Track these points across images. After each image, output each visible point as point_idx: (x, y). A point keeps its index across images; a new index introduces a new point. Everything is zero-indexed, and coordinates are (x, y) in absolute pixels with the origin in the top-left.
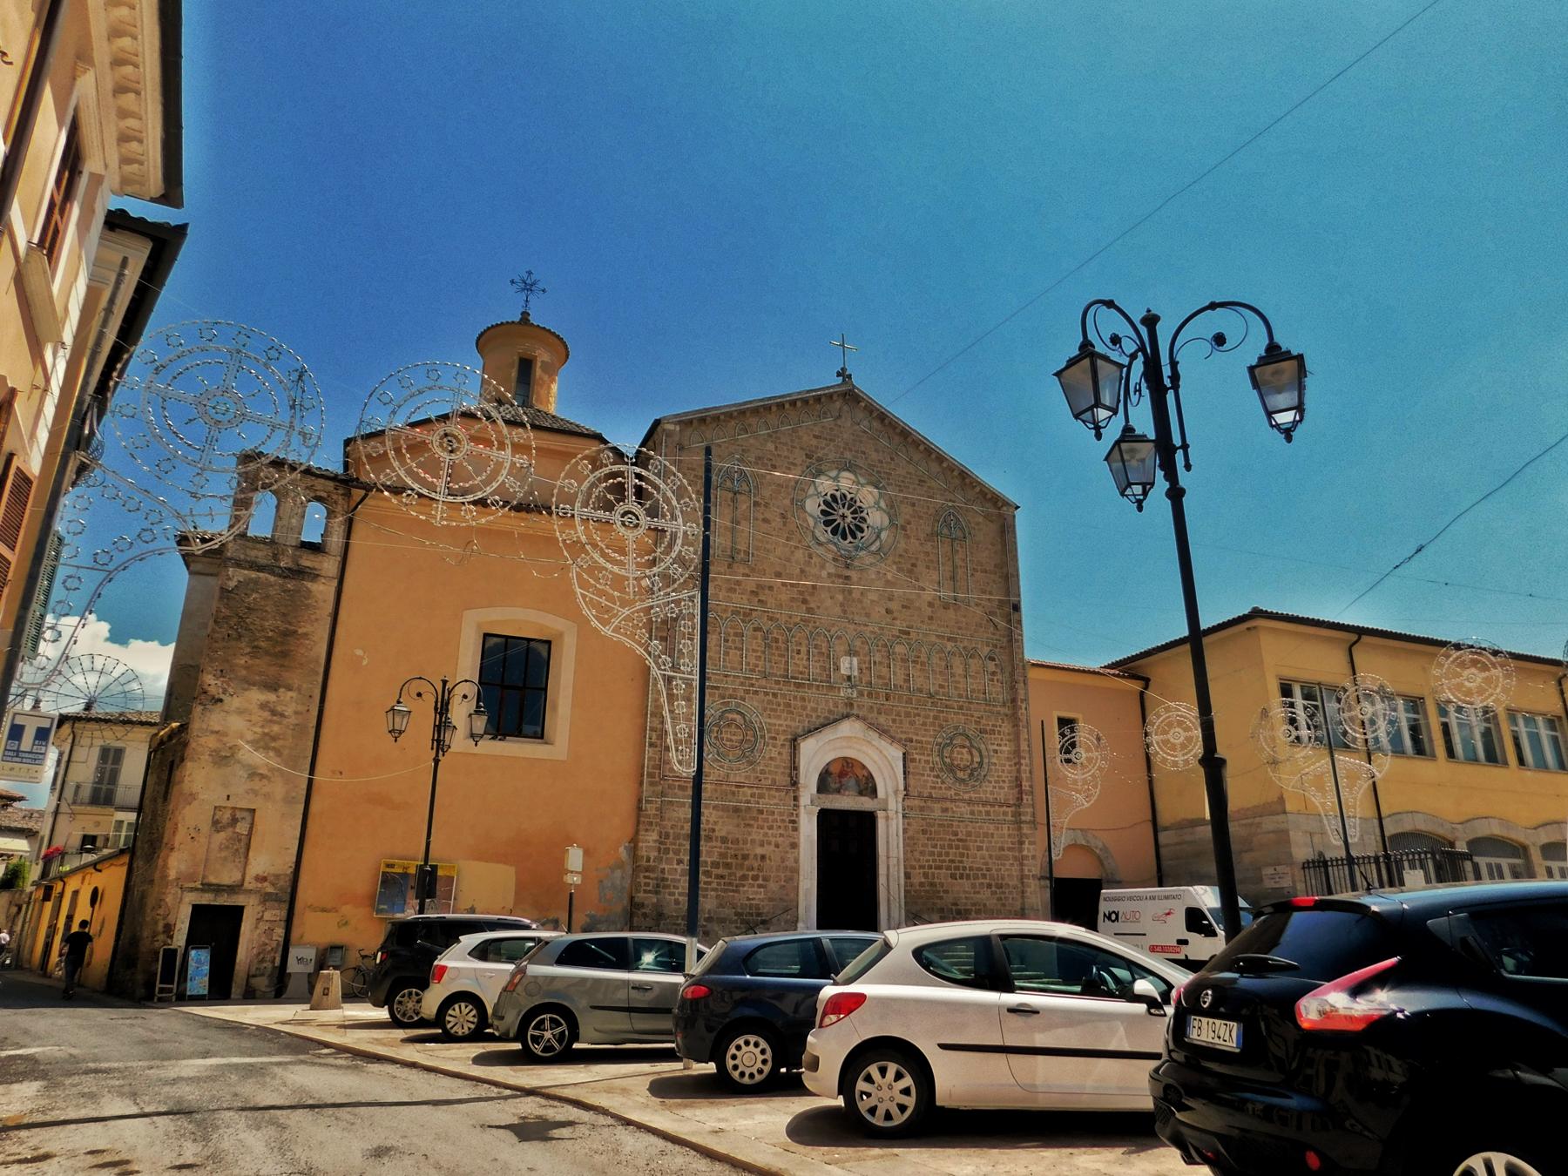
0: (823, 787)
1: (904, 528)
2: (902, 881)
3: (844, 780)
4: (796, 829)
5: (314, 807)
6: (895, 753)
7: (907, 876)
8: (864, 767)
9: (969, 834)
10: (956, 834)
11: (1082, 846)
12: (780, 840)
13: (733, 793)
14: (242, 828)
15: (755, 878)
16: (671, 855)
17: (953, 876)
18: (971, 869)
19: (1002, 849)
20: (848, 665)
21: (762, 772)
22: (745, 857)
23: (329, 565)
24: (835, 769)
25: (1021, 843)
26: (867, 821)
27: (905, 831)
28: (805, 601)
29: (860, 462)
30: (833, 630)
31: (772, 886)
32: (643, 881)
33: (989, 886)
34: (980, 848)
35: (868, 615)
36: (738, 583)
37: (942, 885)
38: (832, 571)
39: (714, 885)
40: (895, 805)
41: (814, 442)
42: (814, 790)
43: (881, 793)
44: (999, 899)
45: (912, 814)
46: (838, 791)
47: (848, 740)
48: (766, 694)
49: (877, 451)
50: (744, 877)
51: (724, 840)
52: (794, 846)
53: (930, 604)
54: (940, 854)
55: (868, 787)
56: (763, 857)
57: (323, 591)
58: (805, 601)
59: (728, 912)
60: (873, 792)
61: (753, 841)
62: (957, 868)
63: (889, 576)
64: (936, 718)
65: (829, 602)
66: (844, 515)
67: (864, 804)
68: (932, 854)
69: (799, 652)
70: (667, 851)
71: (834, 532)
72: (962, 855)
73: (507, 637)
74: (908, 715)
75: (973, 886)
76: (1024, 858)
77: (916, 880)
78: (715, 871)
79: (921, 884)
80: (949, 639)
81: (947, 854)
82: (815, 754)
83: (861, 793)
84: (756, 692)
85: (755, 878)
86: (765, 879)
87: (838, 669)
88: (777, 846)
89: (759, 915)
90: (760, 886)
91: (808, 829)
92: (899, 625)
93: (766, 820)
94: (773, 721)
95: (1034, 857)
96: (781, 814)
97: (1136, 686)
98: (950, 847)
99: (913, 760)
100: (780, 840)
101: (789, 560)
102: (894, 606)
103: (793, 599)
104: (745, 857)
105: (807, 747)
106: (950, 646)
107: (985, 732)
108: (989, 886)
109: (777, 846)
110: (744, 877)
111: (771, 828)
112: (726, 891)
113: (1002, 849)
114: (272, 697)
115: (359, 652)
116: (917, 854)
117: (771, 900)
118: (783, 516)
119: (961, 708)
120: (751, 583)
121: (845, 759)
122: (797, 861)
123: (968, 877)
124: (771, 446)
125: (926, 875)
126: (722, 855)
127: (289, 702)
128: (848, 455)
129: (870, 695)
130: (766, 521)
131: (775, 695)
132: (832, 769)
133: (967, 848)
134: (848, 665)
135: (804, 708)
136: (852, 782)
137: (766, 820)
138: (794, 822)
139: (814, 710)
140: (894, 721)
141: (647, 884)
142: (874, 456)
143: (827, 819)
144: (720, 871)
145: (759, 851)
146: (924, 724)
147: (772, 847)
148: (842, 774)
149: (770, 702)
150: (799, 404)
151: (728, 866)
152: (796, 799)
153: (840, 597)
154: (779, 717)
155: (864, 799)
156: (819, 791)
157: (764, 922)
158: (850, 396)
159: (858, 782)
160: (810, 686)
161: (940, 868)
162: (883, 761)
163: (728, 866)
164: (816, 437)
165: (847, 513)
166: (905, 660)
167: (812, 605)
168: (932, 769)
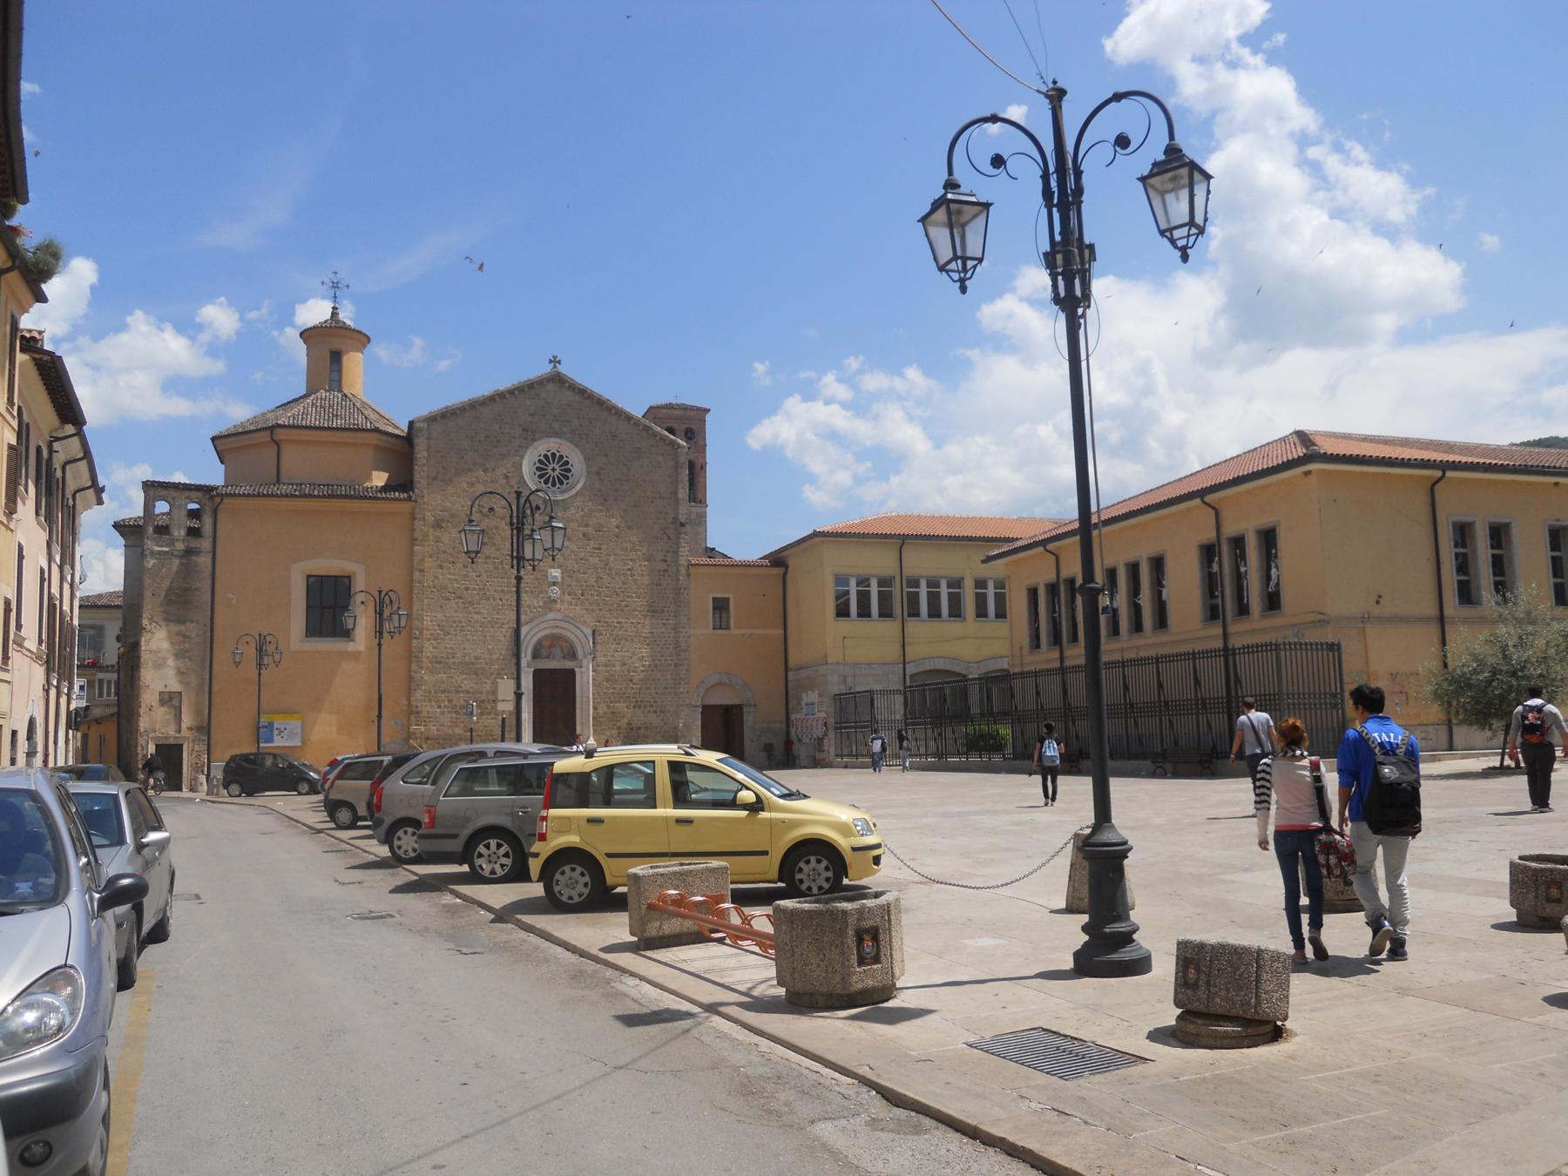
5: (215, 688)
8: (567, 640)
14: (175, 702)
23: (205, 544)
24: (546, 644)
57: (204, 561)
60: (574, 656)
66: (554, 470)
67: (568, 665)
71: (546, 482)
97: (780, 571)
102: (590, 530)
106: (633, 555)
114: (182, 628)
118: (506, 477)
124: (496, 427)
127: (193, 630)
128: (556, 425)
132: (546, 644)
134: (556, 573)
143: (539, 675)
158: (558, 379)
166: (595, 568)
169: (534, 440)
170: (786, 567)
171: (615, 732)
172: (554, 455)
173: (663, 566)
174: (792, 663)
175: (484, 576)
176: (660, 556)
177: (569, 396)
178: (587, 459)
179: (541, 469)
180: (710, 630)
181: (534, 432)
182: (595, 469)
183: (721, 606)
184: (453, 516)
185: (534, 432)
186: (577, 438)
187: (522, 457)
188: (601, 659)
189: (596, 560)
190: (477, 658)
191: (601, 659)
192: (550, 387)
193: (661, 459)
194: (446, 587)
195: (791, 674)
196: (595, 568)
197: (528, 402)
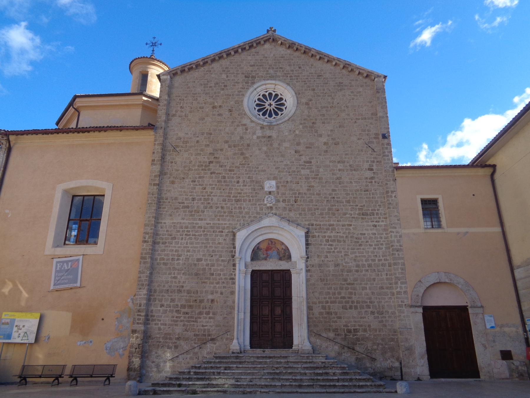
0: (255, 256)
1: (307, 104)
2: (305, 312)
3: (269, 252)
4: (234, 283)
6: (301, 233)
7: (309, 308)
8: (283, 243)
9: (355, 280)
10: (346, 280)
11: (445, 283)
12: (223, 290)
13: (195, 265)
15: (208, 313)
16: (157, 302)
17: (344, 308)
18: (358, 302)
19: (382, 288)
20: (270, 185)
21: (213, 251)
22: (201, 301)
24: (263, 246)
25: (396, 283)
26: (285, 277)
27: (307, 280)
28: (242, 154)
29: (279, 74)
30: (260, 168)
31: (219, 318)
32: (137, 317)
33: (373, 313)
34: (364, 288)
35: (283, 156)
36: (202, 150)
37: (336, 313)
38: (260, 135)
39: (182, 318)
40: (301, 265)
41: (251, 69)
42: (249, 259)
43: (293, 259)
44: (382, 321)
45: (313, 269)
46: (265, 259)
48: (217, 207)
49: (290, 65)
50: (200, 313)
51: (189, 292)
52: (233, 293)
53: (325, 144)
54: (334, 294)
55: (286, 255)
56: (212, 301)
58: (242, 154)
59: (190, 334)
60: (289, 257)
61: (206, 292)
62: (348, 302)
63: (297, 132)
64: (329, 209)
65: (258, 152)
67: (283, 265)
68: (329, 293)
69: (238, 182)
70: (155, 300)
72: (351, 293)
73: (84, 196)
74: (310, 209)
75: (359, 313)
76: (399, 293)
77: (317, 310)
78: (183, 310)
79: (321, 313)
80: (339, 162)
81: (339, 293)
82: (246, 239)
83: (280, 259)
84: (211, 207)
85: (208, 313)
86: (214, 314)
87: (263, 188)
88: (222, 293)
89: (209, 335)
90: (210, 318)
91: (243, 284)
92: (304, 158)
93: (215, 279)
94: (221, 222)
95: (405, 292)
96: (224, 275)
98: (342, 289)
99: (313, 237)
100: (224, 290)
101: (233, 134)
102: (300, 148)
103: (235, 154)
104: (201, 301)
105: (241, 235)
107: (367, 215)
108: (373, 313)
109: (222, 293)
110: (200, 313)
111: (218, 283)
112: (188, 321)
113: (382, 288)
115: (7, 211)
116: (317, 295)
117: (217, 326)
118: (230, 111)
119: (348, 202)
120: (210, 150)
121: (270, 240)
122: (234, 302)
123: (356, 308)
124: (224, 76)
125: (324, 308)
126: (187, 301)
128: (271, 71)
129: (284, 201)
130: (220, 115)
131: (222, 208)
133: (355, 289)
135: (241, 213)
136: (275, 253)
137: (215, 279)
138: (233, 279)
139: (247, 213)
140: (300, 214)
141: (139, 319)
142: (288, 68)
143: (257, 276)
144: (186, 310)
145: (210, 297)
146: (322, 214)
147: (219, 295)
148: (268, 249)
149: (219, 212)
150: (240, 50)
151: (190, 307)
152: (234, 265)
153: (265, 148)
154: (225, 220)
155: (282, 263)
156: (252, 259)
157: (212, 340)
158: (271, 38)
159: (278, 253)
160: (245, 201)
161: (334, 302)
162: (294, 239)
163: (190, 307)
164: (251, 66)
165: (273, 103)
166: (307, 178)
167: (247, 155)
168: (327, 241)
169: (253, 83)
170: (494, 166)
171: (331, 335)
172: (270, 94)
173: (369, 174)
174: (517, 260)
175: (209, 189)
176: (366, 165)
177: (282, 51)
178: (298, 94)
179: (260, 107)
180: (422, 231)
181: (254, 77)
182: (304, 100)
183: (430, 207)
184: (187, 142)
185: (254, 77)
186: (289, 79)
187: (243, 95)
188: (315, 261)
189: (307, 172)
190: (199, 260)
191: (315, 261)
192: (267, 46)
193: (361, 89)
194: (176, 199)
195: (517, 273)
196: (307, 178)
197: (249, 58)
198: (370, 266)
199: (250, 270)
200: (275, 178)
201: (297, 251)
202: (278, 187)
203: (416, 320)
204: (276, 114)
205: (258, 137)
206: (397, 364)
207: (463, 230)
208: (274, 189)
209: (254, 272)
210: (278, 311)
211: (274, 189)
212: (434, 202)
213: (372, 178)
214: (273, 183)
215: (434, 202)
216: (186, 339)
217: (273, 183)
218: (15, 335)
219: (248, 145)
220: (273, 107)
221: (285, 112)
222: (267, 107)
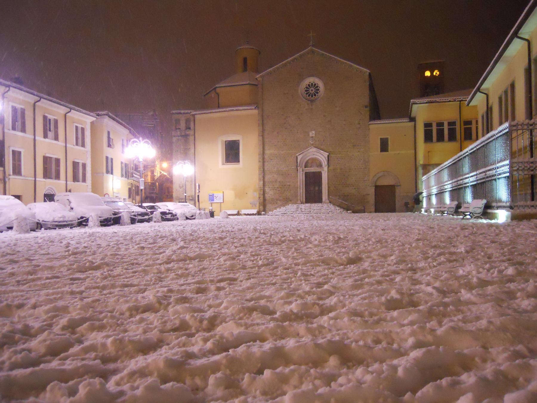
40: (326, 169)
47: (313, 153)
51: (279, 182)
55: (320, 165)
66: (312, 90)
87: (309, 135)
95: (369, 180)
97: (413, 123)
125: (335, 187)
143: (307, 175)
145: (288, 184)
148: (312, 163)
198: (355, 169)
199: (304, 172)
200: (314, 130)
201: (325, 163)
202: (316, 135)
203: (372, 191)
204: (315, 95)
205: (306, 109)
206: (363, 208)
207: (398, 152)
208: (314, 135)
209: (306, 174)
210: (317, 188)
211: (314, 135)
212: (387, 139)
213: (359, 128)
214: (314, 132)
215: (387, 139)
216: (280, 200)
217: (314, 132)
218: (215, 200)
219: (302, 114)
220: (313, 91)
221: (319, 94)
222: (311, 92)
